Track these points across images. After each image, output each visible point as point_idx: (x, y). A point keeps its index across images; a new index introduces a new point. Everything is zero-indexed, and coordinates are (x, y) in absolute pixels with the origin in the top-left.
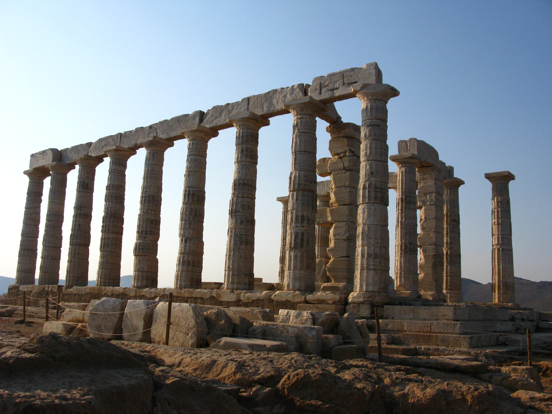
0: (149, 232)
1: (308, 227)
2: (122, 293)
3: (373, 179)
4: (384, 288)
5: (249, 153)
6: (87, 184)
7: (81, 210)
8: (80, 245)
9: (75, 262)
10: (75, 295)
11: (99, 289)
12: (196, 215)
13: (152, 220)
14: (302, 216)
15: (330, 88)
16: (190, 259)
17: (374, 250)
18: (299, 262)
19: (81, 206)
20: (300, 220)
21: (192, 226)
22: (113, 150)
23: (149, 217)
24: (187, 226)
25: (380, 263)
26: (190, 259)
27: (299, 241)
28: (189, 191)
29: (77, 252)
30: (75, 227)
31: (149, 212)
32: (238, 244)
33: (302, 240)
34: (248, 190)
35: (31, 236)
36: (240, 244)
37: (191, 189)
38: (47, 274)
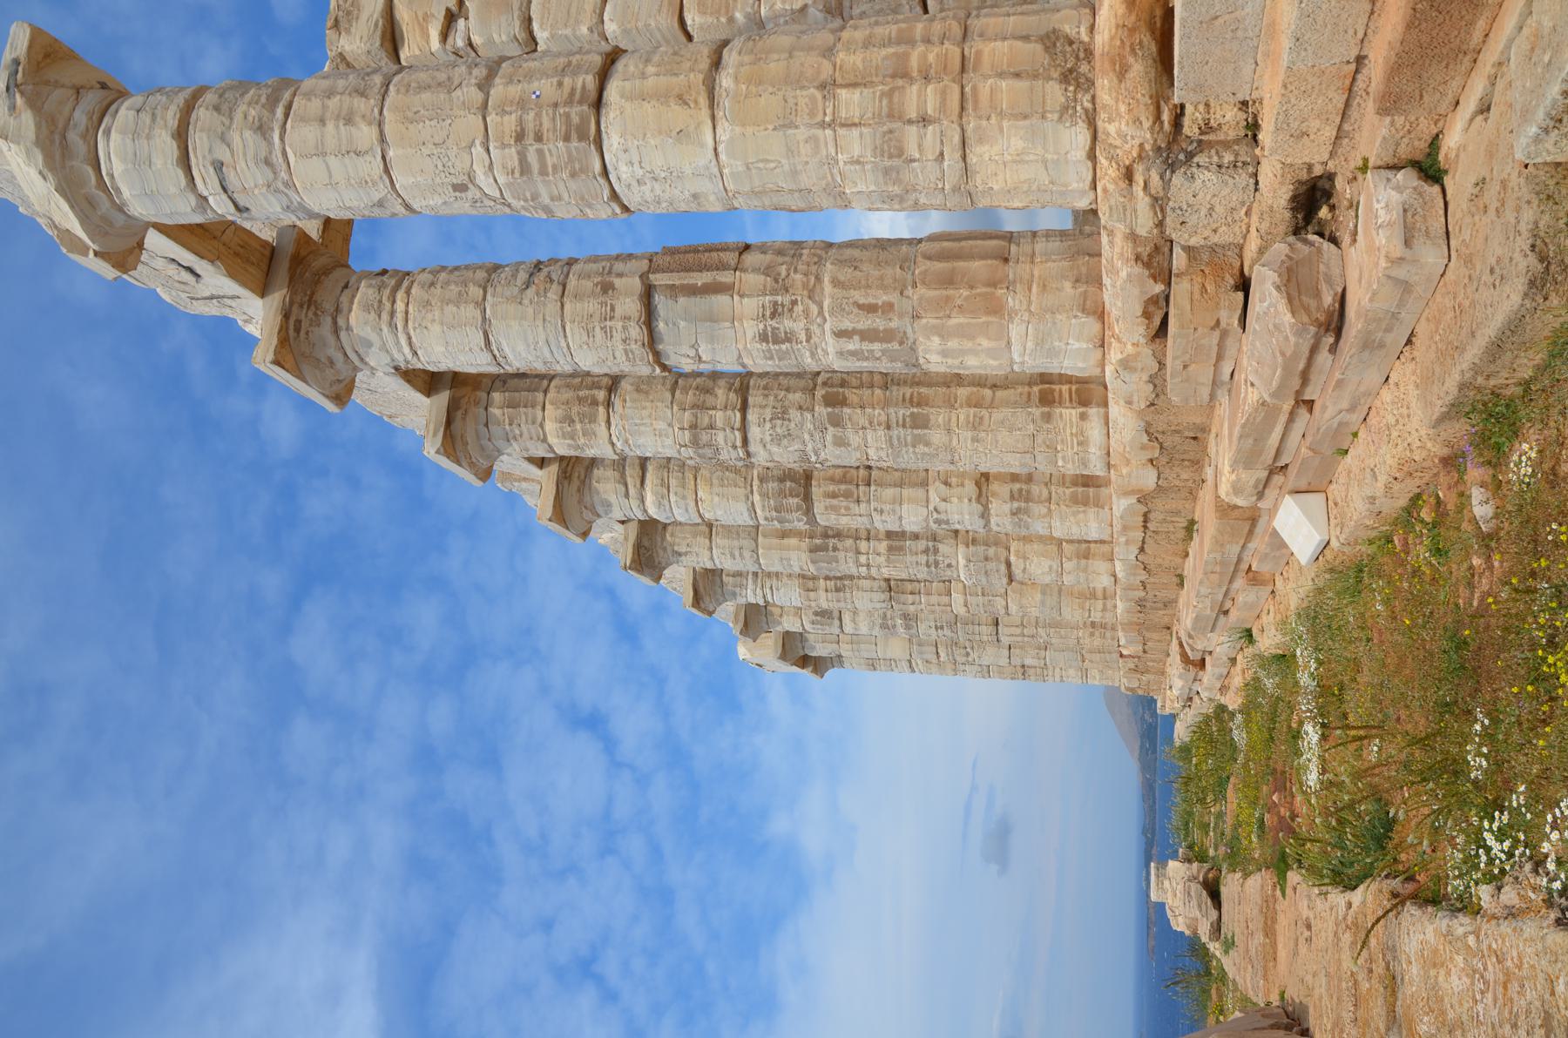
0: (931, 559)
1: (806, 313)
3: (482, 179)
4: (1068, 76)
5: (578, 426)
6: (816, 614)
7: (894, 626)
12: (847, 495)
13: (890, 549)
14: (764, 338)
16: (1007, 508)
17: (858, 162)
18: (969, 345)
20: (784, 347)
21: (887, 507)
23: (882, 559)
25: (924, 120)
26: (1007, 508)
27: (876, 346)
29: (1018, 631)
31: (863, 559)
32: (926, 450)
33: (868, 335)
34: (711, 427)
36: (927, 444)
38: (1087, 656)
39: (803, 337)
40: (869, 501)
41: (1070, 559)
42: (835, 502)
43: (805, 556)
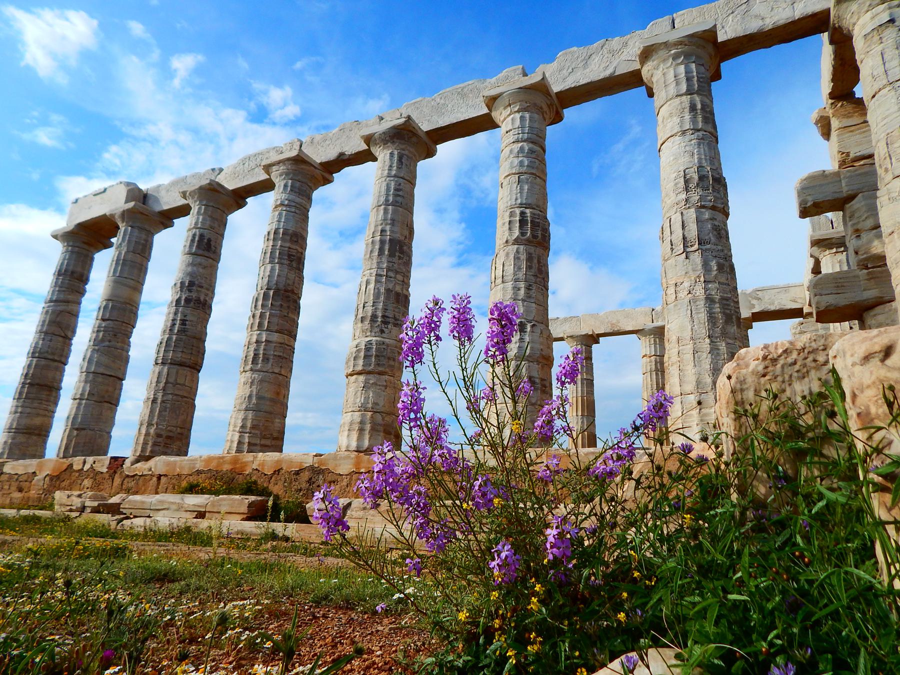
0: (391, 320)
2: (312, 468)
6: (209, 240)
7: (190, 291)
8: (181, 364)
9: (163, 402)
10: (159, 477)
11: (235, 461)
19: (191, 284)
22: (288, 159)
23: (391, 286)
24: (522, 292)
28: (522, 214)
29: (171, 380)
30: (173, 325)
35: (50, 357)
37: (528, 211)
38: (83, 432)
40: (536, 283)
41: (383, 419)
42: (535, 261)
43: (398, 236)
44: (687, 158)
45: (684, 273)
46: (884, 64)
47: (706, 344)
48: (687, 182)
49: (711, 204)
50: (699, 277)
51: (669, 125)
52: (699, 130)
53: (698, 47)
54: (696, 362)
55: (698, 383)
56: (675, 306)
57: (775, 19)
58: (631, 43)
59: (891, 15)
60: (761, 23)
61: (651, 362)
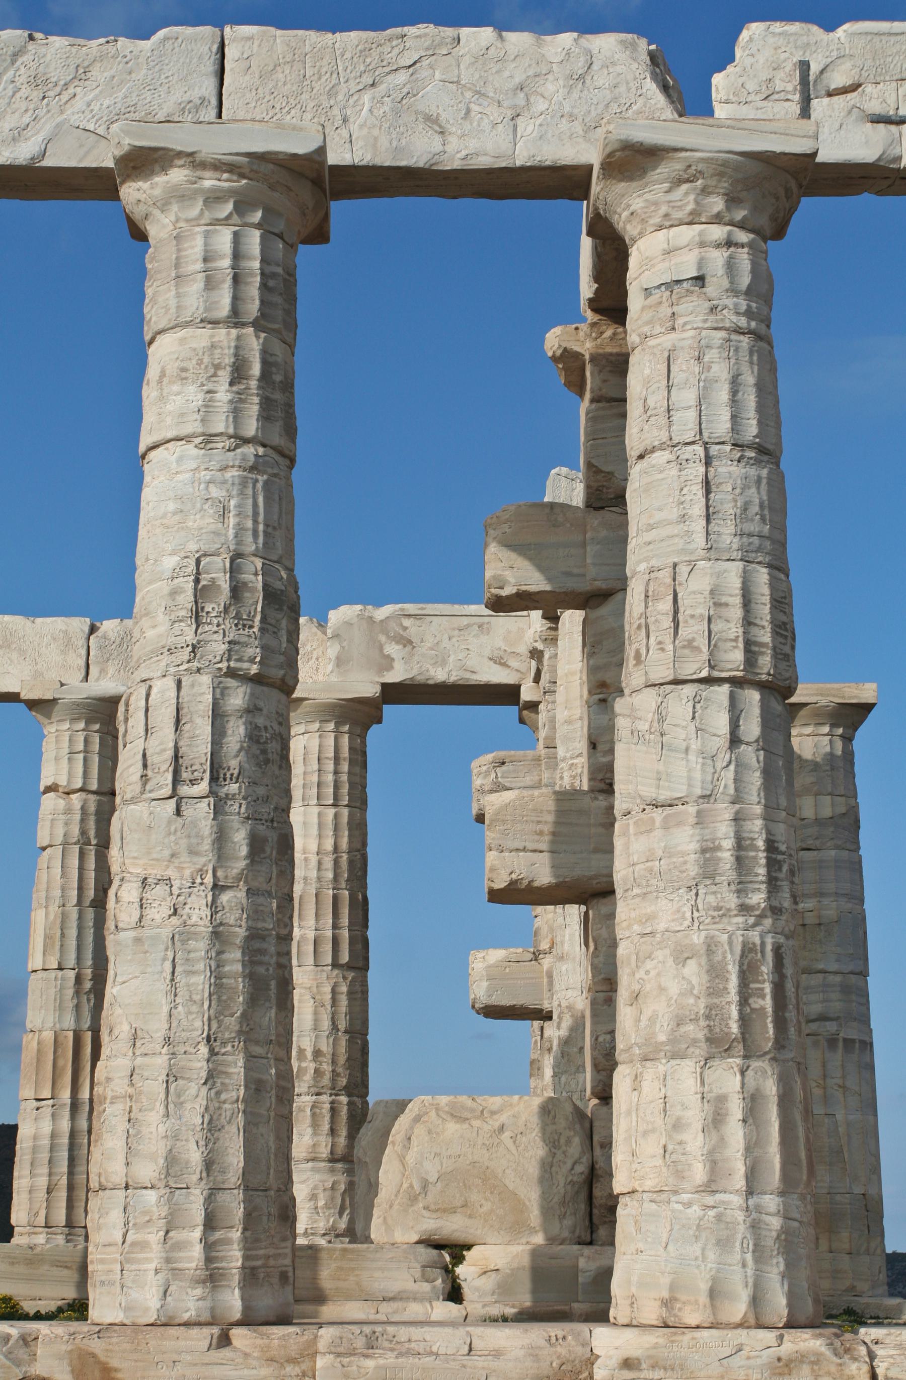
15: (875, 107)
39: (775, 903)
44: (207, 520)
45: (167, 853)
46: (669, 388)
47: (198, 1062)
48: (201, 592)
49: (254, 669)
50: (202, 872)
51: (175, 404)
52: (246, 441)
53: (272, 188)
54: (172, 1103)
55: (172, 1161)
56: (138, 940)
57: (473, 145)
58: (98, 74)
59: (701, 264)
60: (436, 144)
61: (68, 811)
